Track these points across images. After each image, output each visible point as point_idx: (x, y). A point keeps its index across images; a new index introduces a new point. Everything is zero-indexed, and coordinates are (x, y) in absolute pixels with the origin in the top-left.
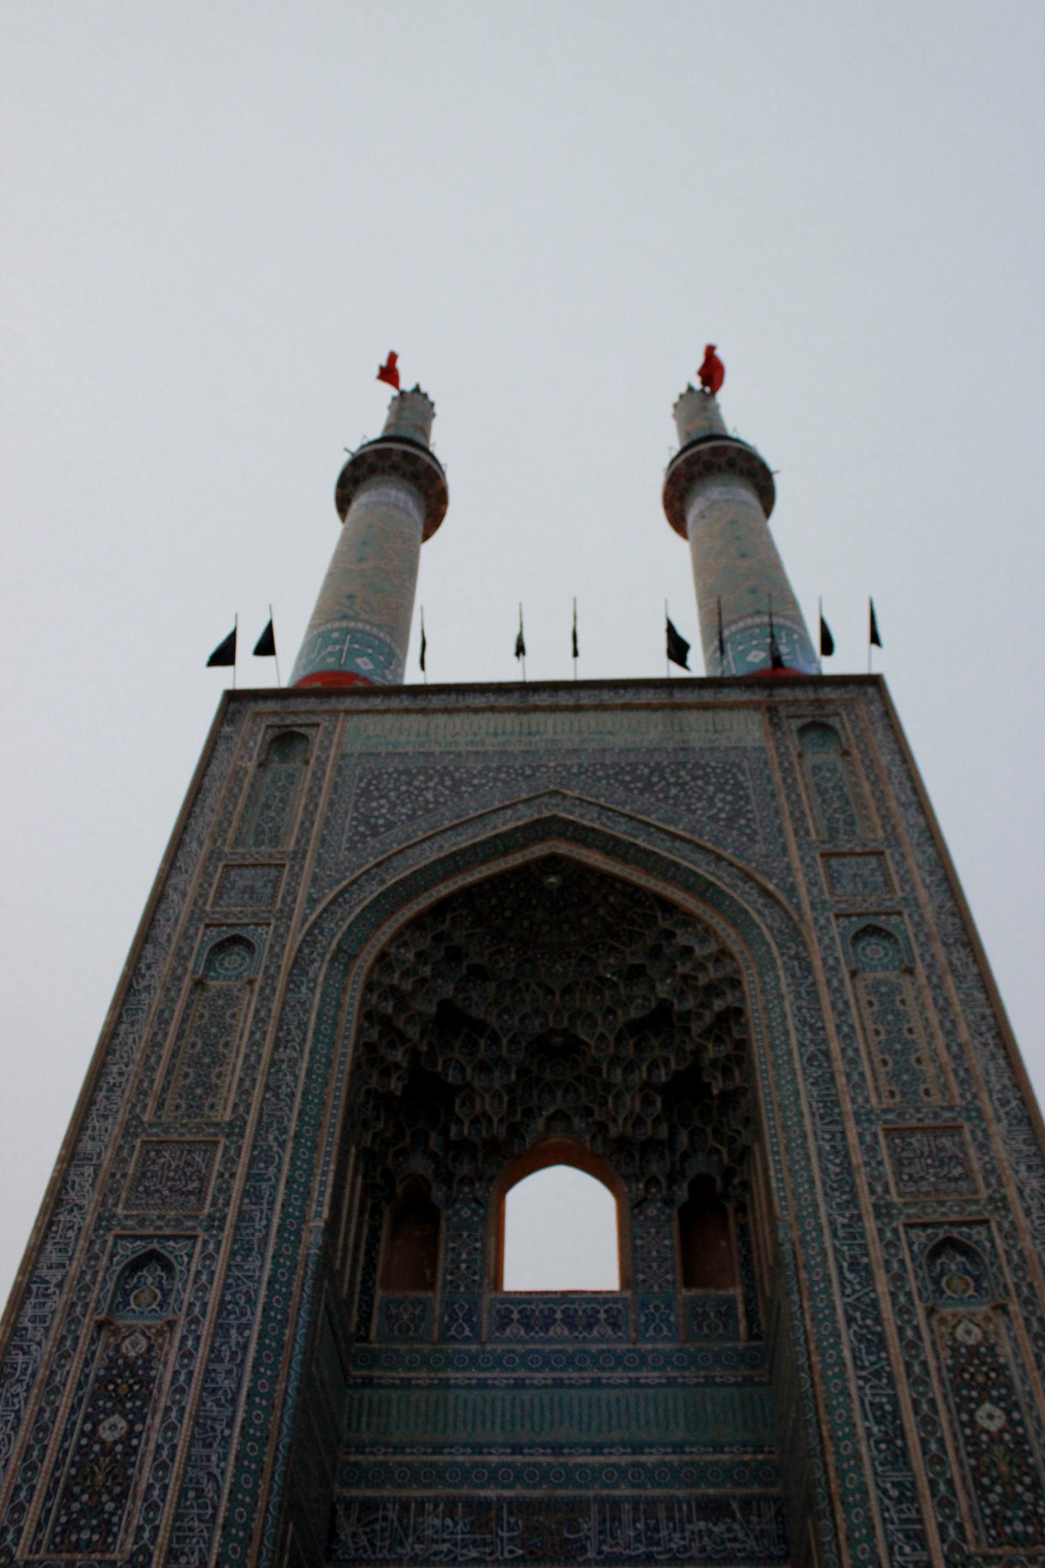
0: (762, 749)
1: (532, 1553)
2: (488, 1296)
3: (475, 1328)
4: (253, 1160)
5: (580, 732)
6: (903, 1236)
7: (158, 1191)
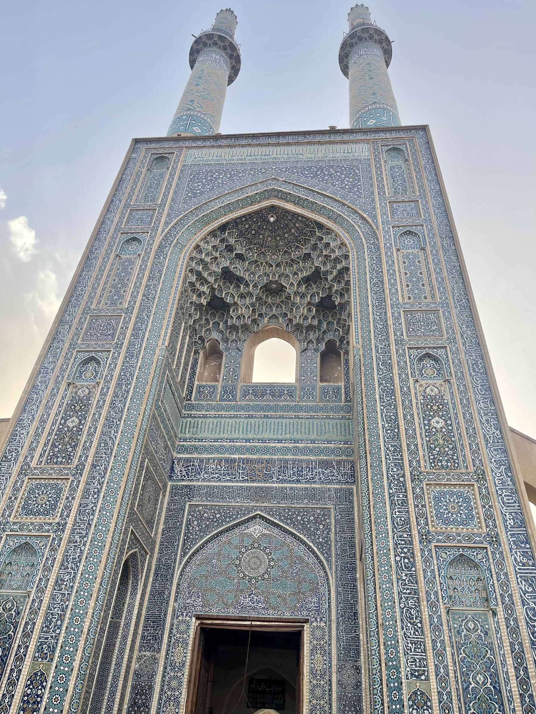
0: (368, 160)
1: (251, 478)
2: (240, 385)
3: (235, 397)
4: (136, 322)
5: (288, 154)
6: (407, 352)
7: (96, 334)
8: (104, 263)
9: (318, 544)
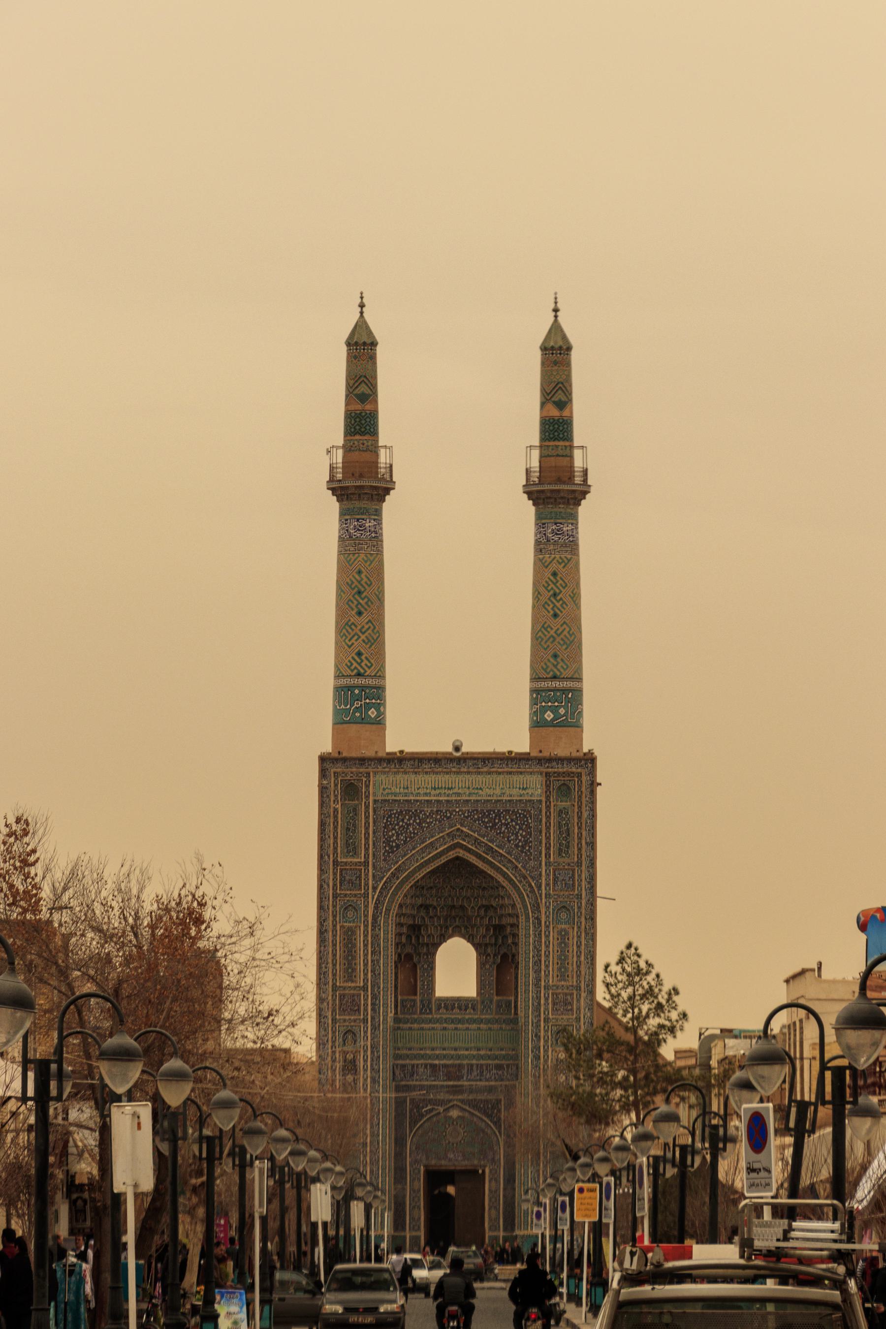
0: (540, 801)
4: (372, 998)
8: (334, 936)
9: (495, 1123)
